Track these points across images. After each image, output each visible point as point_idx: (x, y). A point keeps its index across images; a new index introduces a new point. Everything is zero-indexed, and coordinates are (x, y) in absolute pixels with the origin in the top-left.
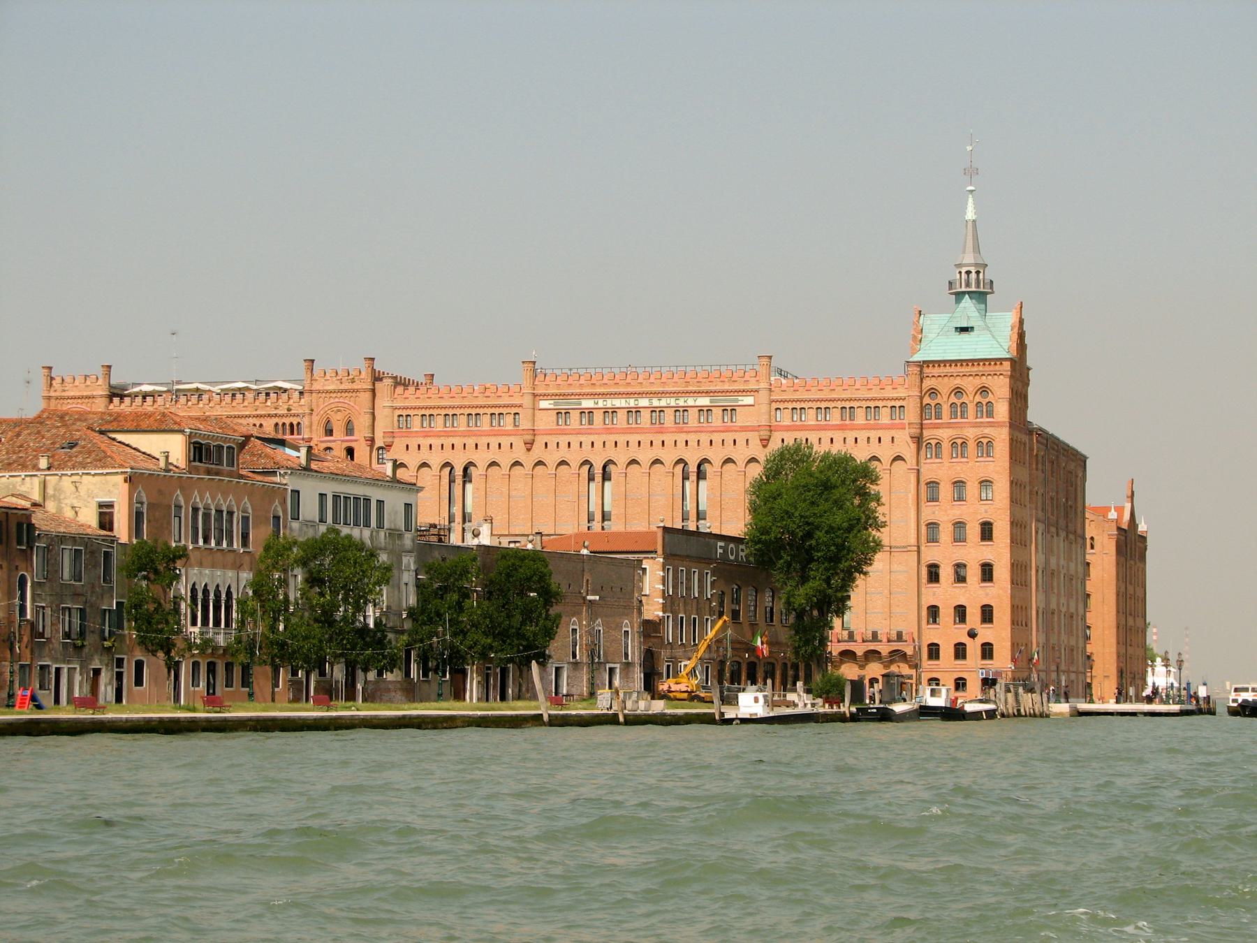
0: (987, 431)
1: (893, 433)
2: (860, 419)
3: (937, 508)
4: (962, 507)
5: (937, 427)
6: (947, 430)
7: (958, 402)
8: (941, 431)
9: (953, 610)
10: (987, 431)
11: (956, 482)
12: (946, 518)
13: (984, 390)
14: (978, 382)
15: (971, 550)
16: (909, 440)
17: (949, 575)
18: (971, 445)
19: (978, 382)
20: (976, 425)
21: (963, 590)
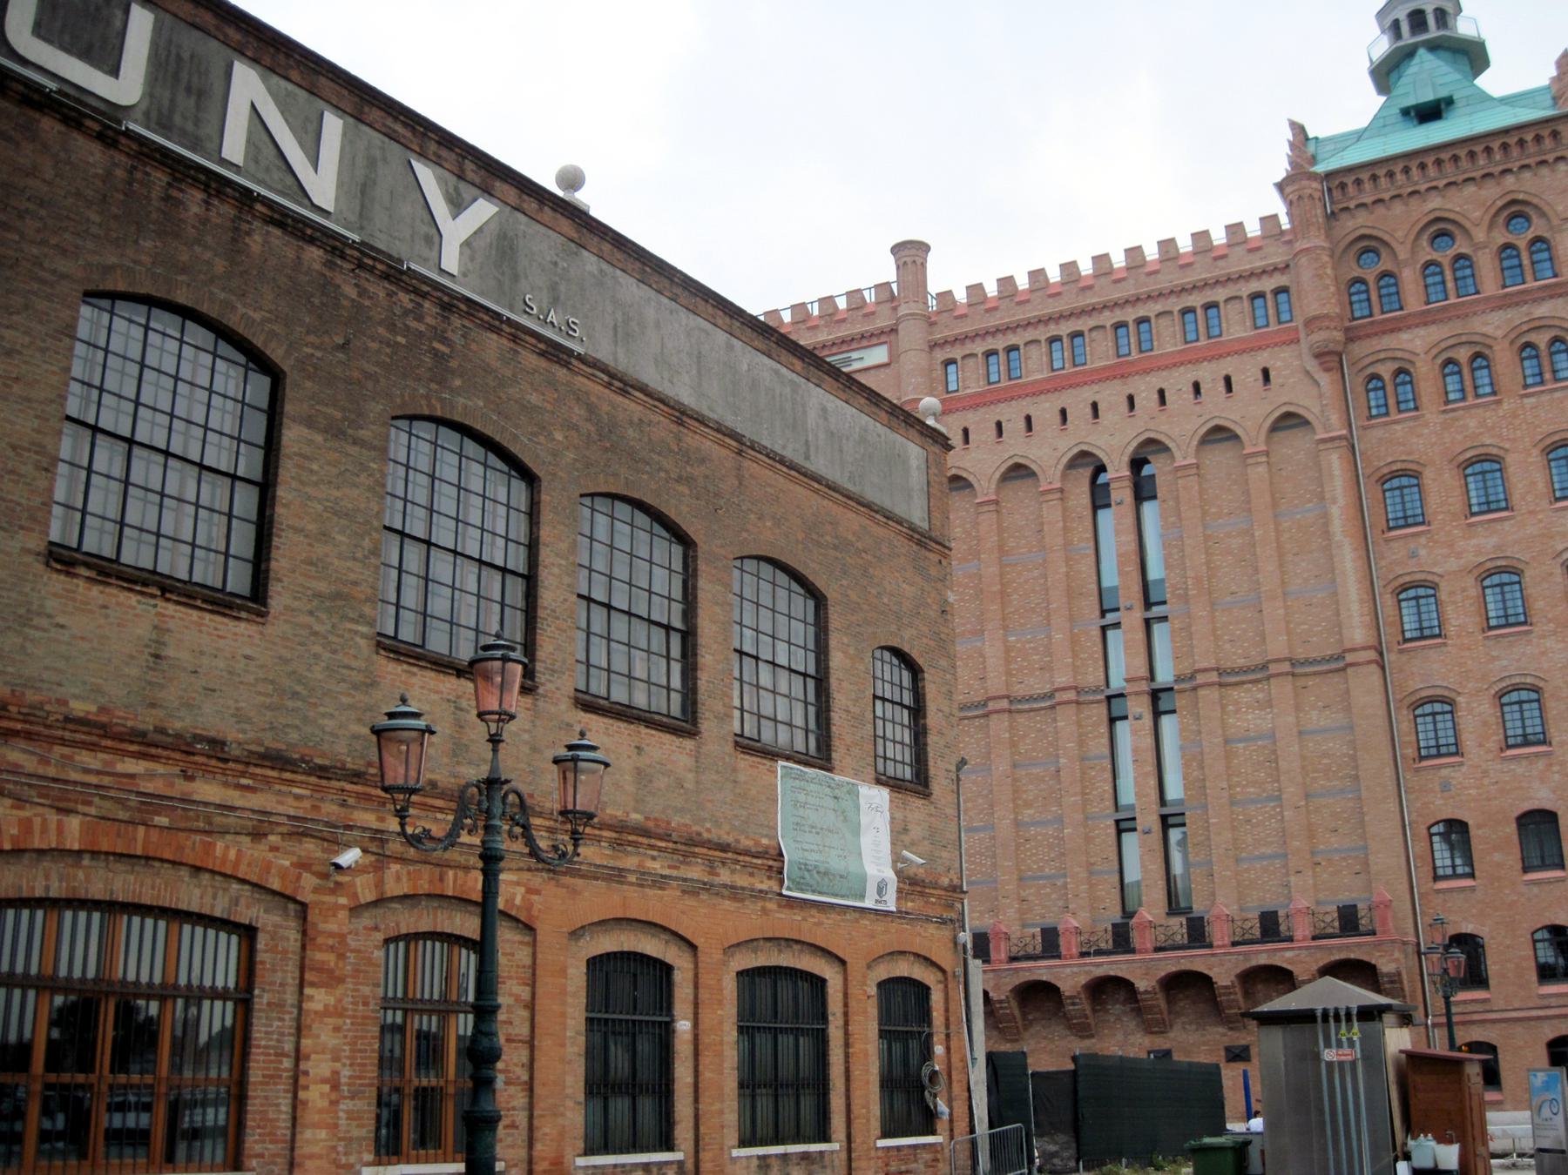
0: (1543, 310)
1: (1264, 358)
2: (1168, 340)
3: (1423, 540)
4: (1498, 526)
5: (1394, 327)
6: (1422, 331)
7: (1445, 256)
8: (1405, 336)
9: (1514, 826)
10: (1543, 310)
11: (1470, 463)
12: (1453, 564)
13: (1516, 211)
14: (1492, 193)
15: (1549, 643)
16: (1312, 365)
17: (1485, 723)
18: (1504, 357)
19: (1492, 193)
20: (1505, 303)
21: (1541, 764)
